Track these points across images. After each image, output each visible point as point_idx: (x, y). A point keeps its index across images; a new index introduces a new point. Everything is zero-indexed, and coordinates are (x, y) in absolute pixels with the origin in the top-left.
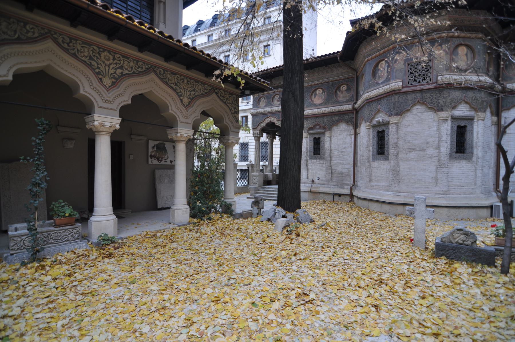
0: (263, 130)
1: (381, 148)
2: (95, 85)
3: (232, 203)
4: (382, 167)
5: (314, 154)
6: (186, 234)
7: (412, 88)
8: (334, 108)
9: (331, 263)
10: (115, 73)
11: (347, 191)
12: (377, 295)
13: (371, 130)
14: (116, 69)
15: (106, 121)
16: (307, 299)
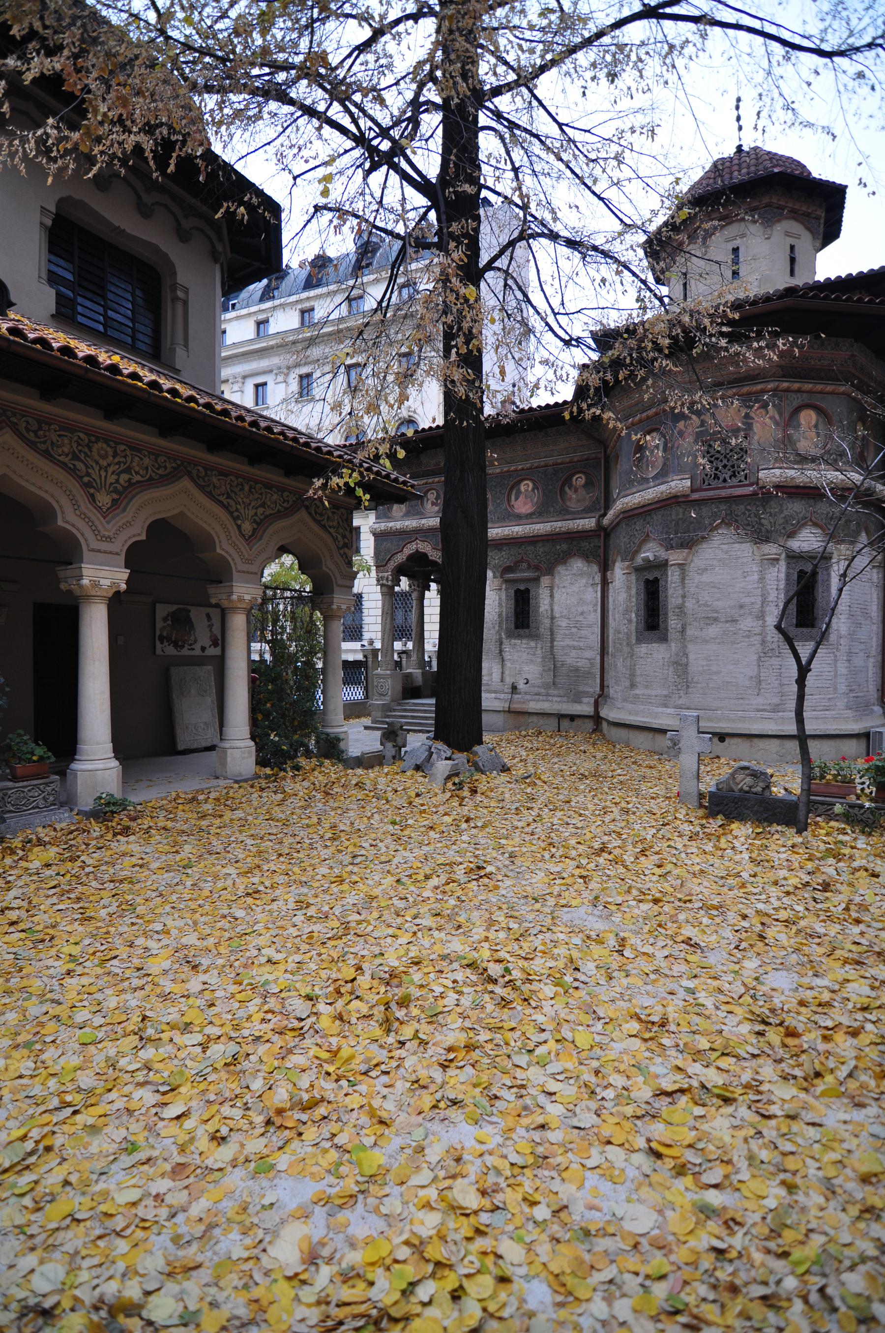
0: (400, 571)
1: (653, 618)
2: (83, 508)
3: (342, 736)
4: (654, 656)
5: (517, 627)
6: (255, 795)
7: (711, 493)
8: (559, 524)
9: (527, 829)
10: (117, 481)
11: (586, 708)
12: (592, 866)
13: (633, 577)
14: (118, 474)
15: (102, 575)
16: (482, 873)
